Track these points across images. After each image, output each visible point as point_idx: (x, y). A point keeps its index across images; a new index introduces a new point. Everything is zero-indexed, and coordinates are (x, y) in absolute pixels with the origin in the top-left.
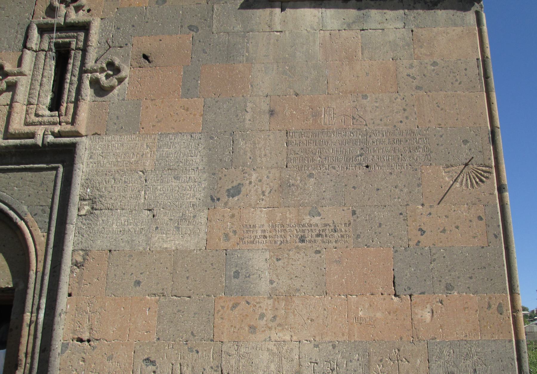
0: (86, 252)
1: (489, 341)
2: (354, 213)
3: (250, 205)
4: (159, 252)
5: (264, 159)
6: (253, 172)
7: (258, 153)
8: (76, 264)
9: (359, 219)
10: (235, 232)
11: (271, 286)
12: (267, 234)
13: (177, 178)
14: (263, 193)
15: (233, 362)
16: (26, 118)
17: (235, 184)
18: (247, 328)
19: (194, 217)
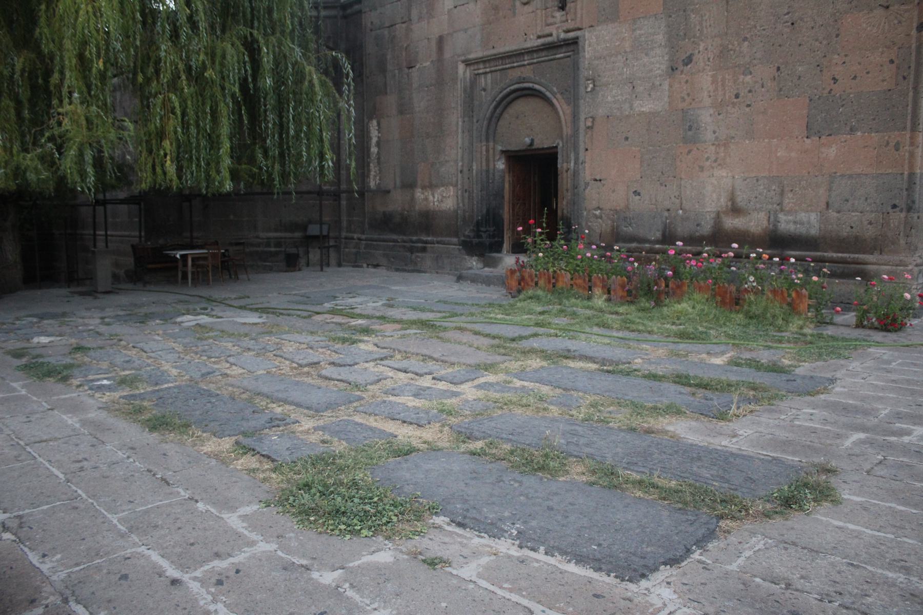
0: (593, 118)
1: (882, 174)
2: (778, 69)
3: (699, 71)
4: (638, 115)
5: (709, 30)
6: (701, 43)
7: (704, 24)
8: (588, 128)
9: (782, 75)
10: (688, 95)
11: (714, 136)
12: (712, 94)
13: (647, 54)
14: (709, 59)
15: (688, 192)
16: (545, 21)
17: (688, 54)
18: (697, 168)
19: (660, 85)
